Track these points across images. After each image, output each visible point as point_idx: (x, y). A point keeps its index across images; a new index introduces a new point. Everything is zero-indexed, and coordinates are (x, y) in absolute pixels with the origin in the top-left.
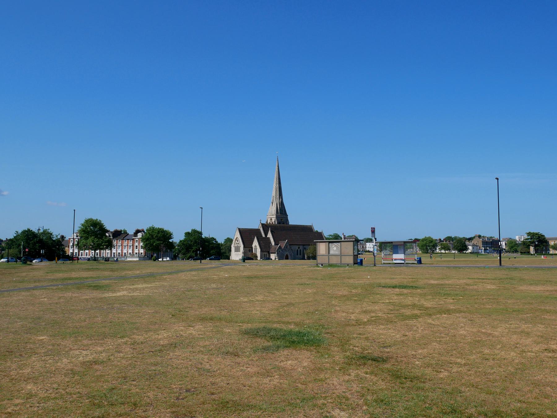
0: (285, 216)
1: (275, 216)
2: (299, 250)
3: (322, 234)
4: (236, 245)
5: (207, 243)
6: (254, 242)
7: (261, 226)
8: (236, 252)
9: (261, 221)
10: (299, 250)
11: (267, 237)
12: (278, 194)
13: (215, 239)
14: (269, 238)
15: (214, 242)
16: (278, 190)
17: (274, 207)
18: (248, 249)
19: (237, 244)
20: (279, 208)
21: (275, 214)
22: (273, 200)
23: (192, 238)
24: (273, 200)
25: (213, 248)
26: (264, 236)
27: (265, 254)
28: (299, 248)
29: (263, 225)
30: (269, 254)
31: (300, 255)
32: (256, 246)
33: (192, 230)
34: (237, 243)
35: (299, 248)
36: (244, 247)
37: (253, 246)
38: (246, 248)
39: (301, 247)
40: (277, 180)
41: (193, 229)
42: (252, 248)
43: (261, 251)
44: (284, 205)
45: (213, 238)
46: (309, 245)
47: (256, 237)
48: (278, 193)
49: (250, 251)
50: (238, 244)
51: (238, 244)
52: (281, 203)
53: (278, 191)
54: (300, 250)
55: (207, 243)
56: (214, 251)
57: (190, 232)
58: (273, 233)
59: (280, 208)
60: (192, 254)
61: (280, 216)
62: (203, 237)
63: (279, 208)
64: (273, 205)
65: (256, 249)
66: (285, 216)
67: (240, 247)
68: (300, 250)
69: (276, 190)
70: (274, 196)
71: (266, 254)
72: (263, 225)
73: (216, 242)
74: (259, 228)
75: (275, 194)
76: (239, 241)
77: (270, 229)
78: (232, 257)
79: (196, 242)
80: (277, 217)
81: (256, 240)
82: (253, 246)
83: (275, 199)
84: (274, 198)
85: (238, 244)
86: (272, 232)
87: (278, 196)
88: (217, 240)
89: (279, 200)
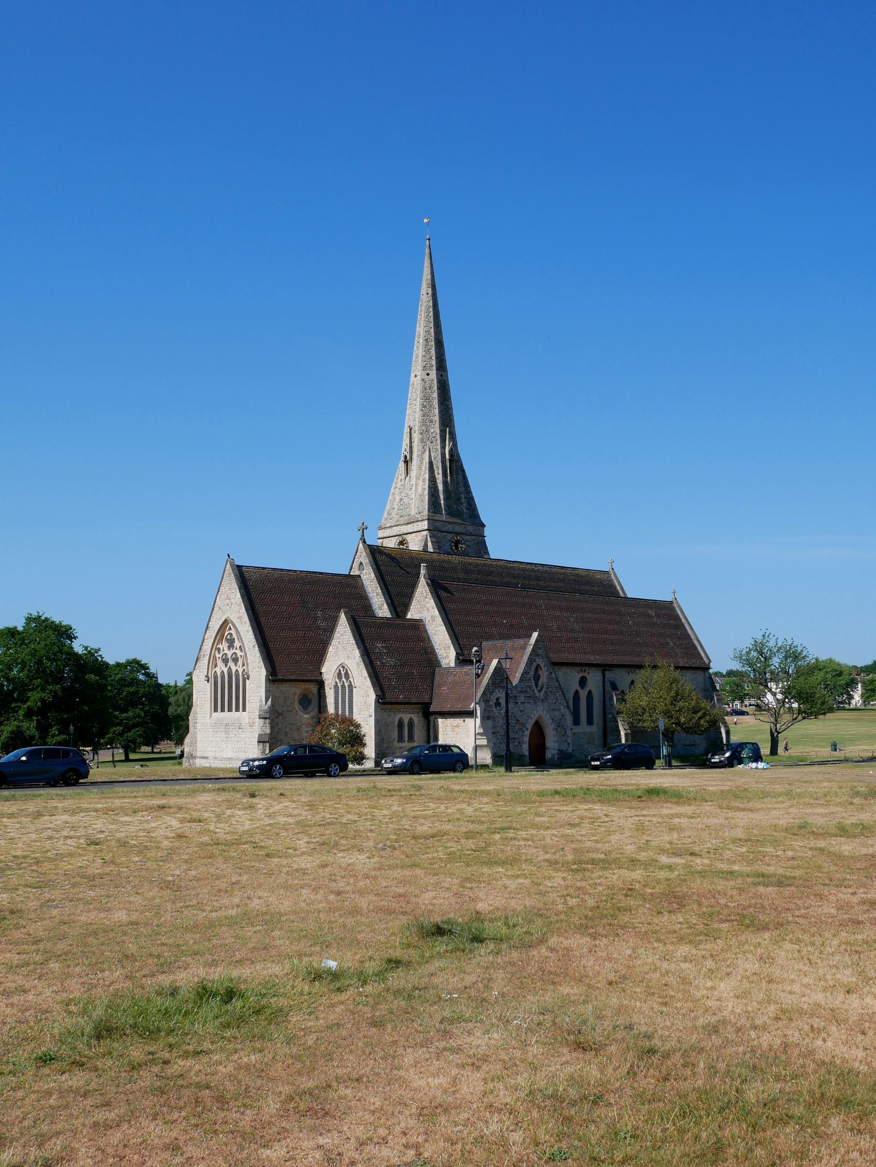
0: (471, 529)
1: (425, 525)
2: (583, 694)
3: (674, 609)
4: (221, 668)
5: (92, 677)
6: (331, 649)
7: (363, 557)
8: (219, 715)
9: (363, 529)
10: (583, 694)
11: (409, 616)
12: (437, 418)
13: (144, 667)
14: (418, 626)
15: (141, 677)
16: (435, 395)
17: (418, 478)
18: (294, 691)
19: (225, 661)
20: (440, 487)
21: (426, 512)
22: (411, 447)
23: (24, 653)
24: (411, 447)
25: (133, 701)
26: (382, 609)
27: (406, 718)
28: (583, 682)
29: (376, 553)
30: (429, 716)
31: (590, 722)
32: (343, 673)
33: (29, 620)
34: (229, 654)
35: (583, 682)
36: (274, 677)
37: (323, 670)
38: (286, 688)
39: (594, 679)
40: (427, 351)
41: (34, 614)
42: (321, 684)
43: (383, 702)
44: (463, 471)
45: (137, 662)
46: (640, 667)
47: (343, 619)
48: (437, 411)
49: (305, 702)
50: (231, 664)
51: (235, 660)
52: (451, 461)
53: (436, 403)
54: (590, 692)
55: (92, 677)
56: (138, 711)
57: (20, 629)
58: (443, 594)
59: (445, 483)
60: (25, 725)
61: (450, 527)
62: (78, 647)
63: (440, 487)
64: (413, 473)
65: (346, 691)
66: (471, 529)
67: (246, 677)
68: (590, 692)
69: (426, 398)
70: (417, 428)
71: (411, 724)
72: (376, 553)
73: (150, 676)
74: (355, 572)
75: (418, 415)
76: (237, 644)
77: (423, 571)
78: (194, 744)
79: (40, 671)
80: (433, 530)
81: (343, 634)
82: (329, 671)
83: (422, 441)
84: (416, 437)
85: (235, 660)
86: (437, 588)
87: (436, 428)
88: (152, 670)
89: (443, 447)
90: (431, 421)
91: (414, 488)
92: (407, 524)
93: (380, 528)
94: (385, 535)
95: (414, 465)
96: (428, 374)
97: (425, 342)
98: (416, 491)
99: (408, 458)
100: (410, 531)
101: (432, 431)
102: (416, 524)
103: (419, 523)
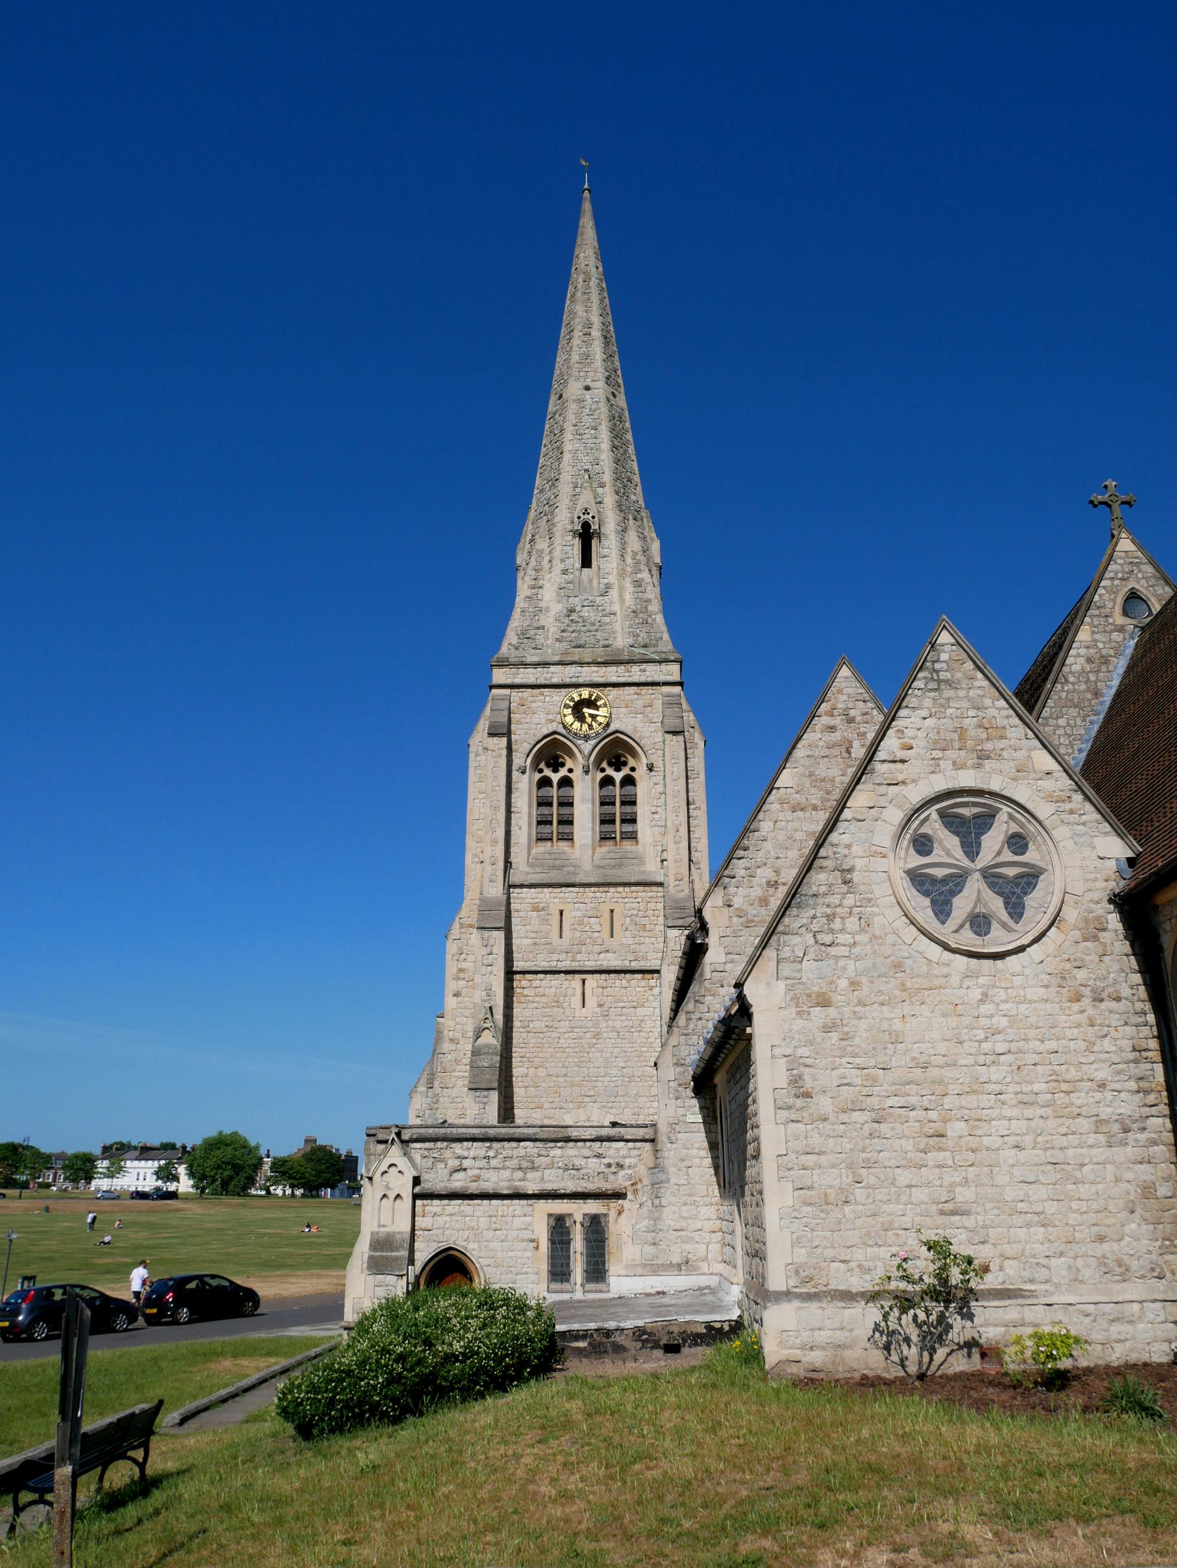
17: (622, 574)
83: (620, 507)
90: (629, 480)
91: (614, 593)
92: (606, 663)
93: (504, 663)
94: (517, 681)
95: (607, 549)
96: (614, 395)
97: (602, 339)
98: (622, 600)
99: (595, 527)
100: (614, 679)
101: (633, 497)
102: (635, 668)
103: (650, 668)
